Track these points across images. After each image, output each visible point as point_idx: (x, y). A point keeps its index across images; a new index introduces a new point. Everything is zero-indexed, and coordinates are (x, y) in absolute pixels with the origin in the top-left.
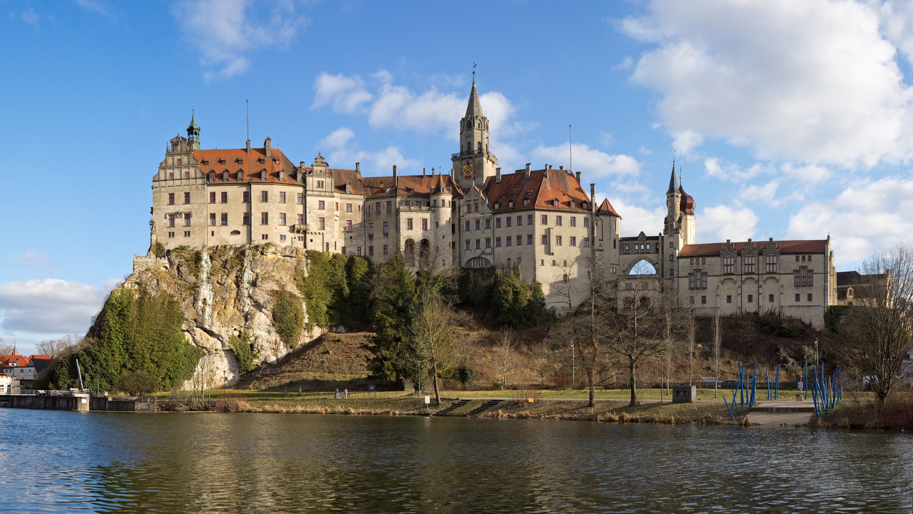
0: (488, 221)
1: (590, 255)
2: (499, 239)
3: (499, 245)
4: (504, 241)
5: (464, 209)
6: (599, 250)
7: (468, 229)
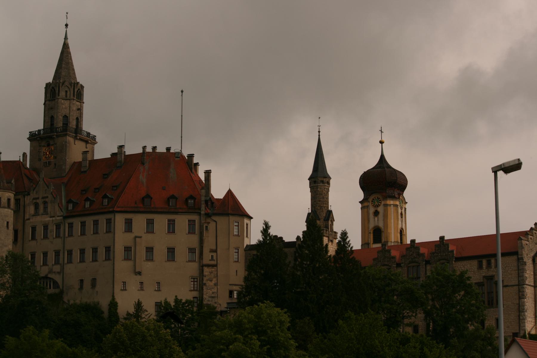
0: (58, 227)
1: (196, 273)
2: (70, 253)
3: (70, 261)
4: (76, 255)
5: (31, 209)
6: (208, 266)
7: (33, 238)
